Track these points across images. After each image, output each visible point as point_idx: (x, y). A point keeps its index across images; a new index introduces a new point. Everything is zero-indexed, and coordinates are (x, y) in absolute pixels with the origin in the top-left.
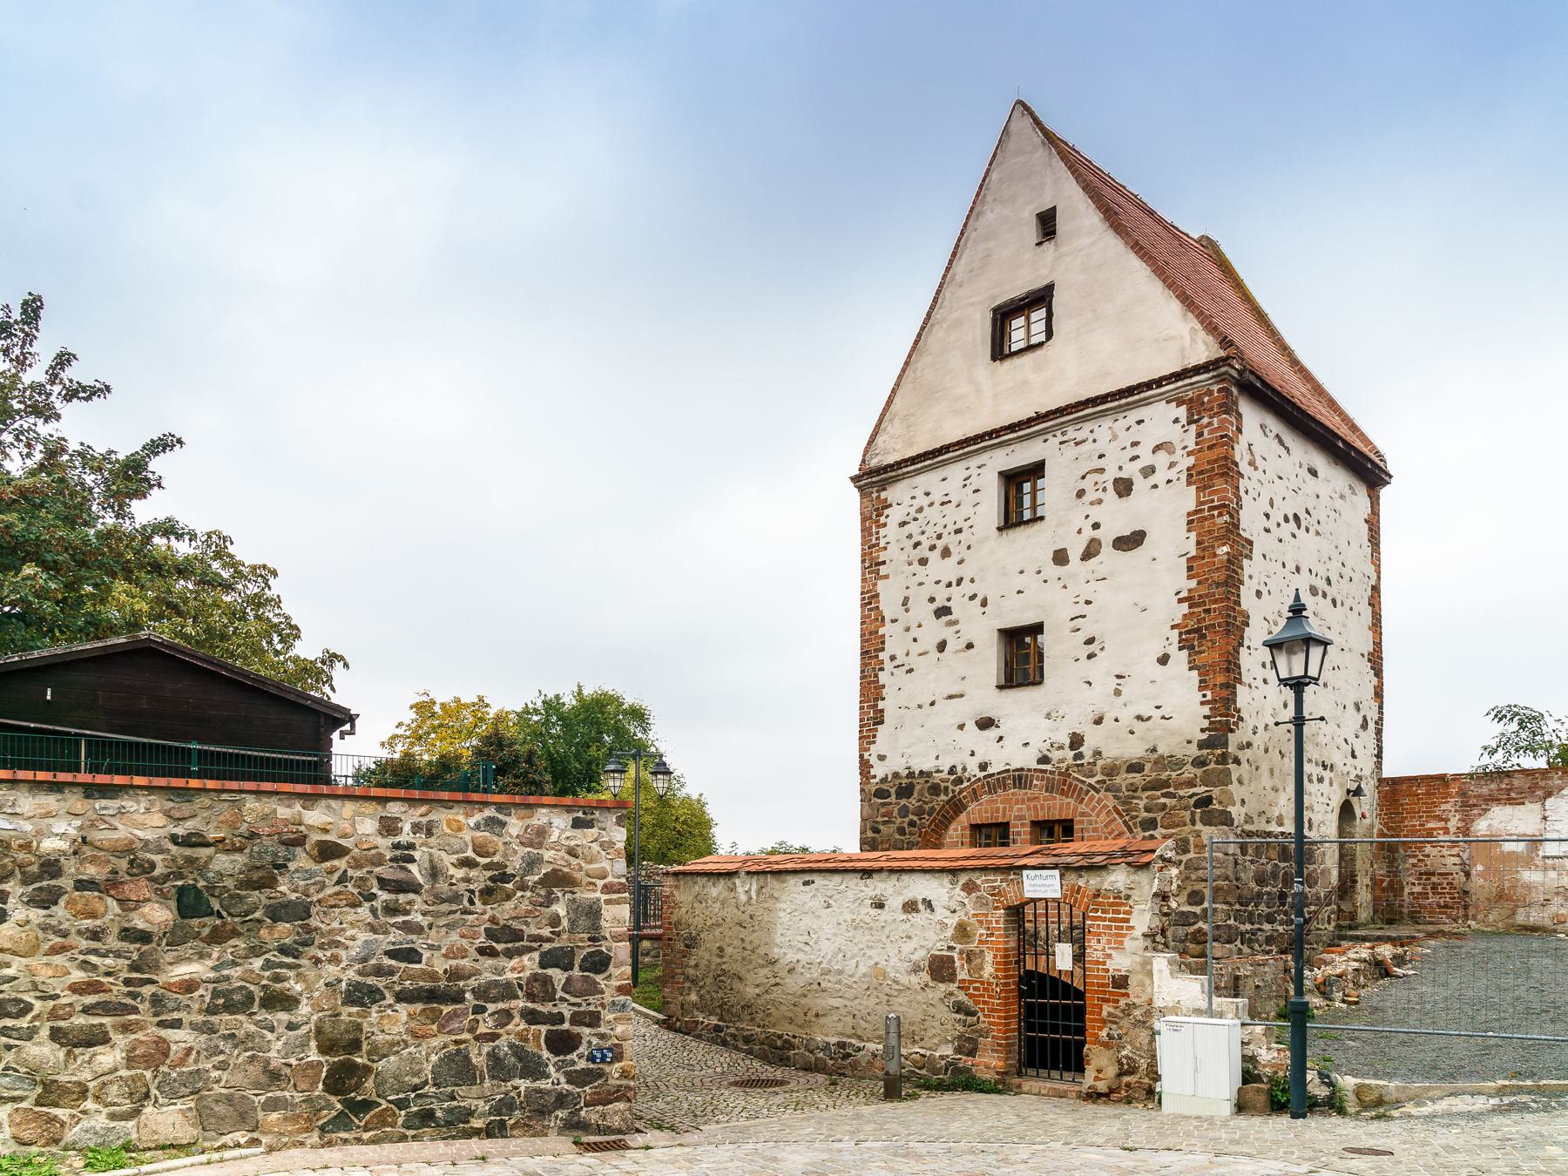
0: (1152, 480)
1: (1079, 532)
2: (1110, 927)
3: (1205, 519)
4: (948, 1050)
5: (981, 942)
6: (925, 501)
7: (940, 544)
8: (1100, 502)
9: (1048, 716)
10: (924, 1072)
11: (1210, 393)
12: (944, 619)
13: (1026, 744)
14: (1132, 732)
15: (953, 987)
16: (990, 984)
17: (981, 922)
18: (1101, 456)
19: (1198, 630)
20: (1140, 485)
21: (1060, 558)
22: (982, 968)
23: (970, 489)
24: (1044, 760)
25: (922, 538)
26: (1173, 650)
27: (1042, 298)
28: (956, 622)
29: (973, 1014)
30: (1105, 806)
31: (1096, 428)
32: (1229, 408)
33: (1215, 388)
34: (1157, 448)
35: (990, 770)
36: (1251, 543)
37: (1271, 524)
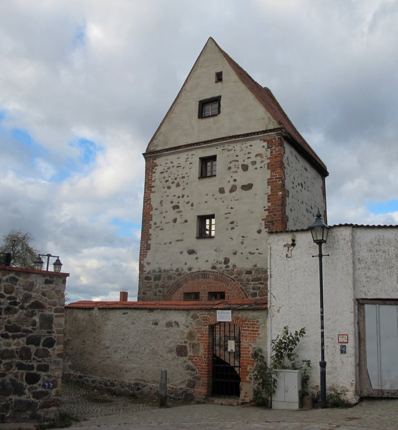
0: (255, 166)
1: (229, 182)
2: (250, 334)
3: (274, 182)
4: (183, 386)
5: (198, 340)
6: (171, 165)
7: (176, 181)
8: (236, 172)
9: (216, 250)
10: (173, 395)
11: (275, 139)
12: (176, 210)
13: (207, 261)
14: (248, 259)
15: (185, 358)
16: (201, 357)
17: (198, 331)
18: (237, 156)
19: (272, 222)
20: (251, 167)
21: (222, 191)
22: (198, 351)
23: (188, 163)
24: (214, 268)
25: (169, 179)
26: (263, 228)
27: (217, 100)
28: (181, 212)
29: (194, 370)
30: (237, 287)
31: (235, 146)
32: (281, 145)
33: (277, 137)
34: (257, 155)
35: (193, 271)
36: (288, 192)
37: (294, 186)
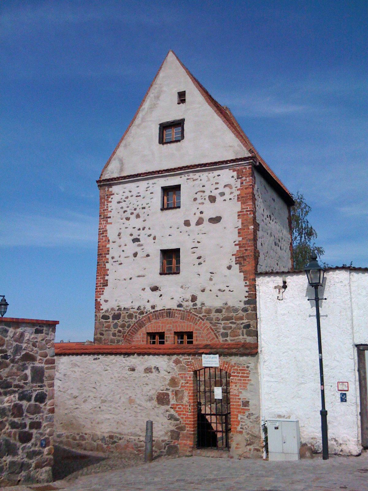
0: (224, 198)
7: (135, 213)
8: (203, 203)
9: (182, 287)
12: (137, 243)
14: (217, 296)
18: (203, 186)
19: (243, 257)
20: (219, 199)
21: (187, 223)
23: (149, 192)
24: (180, 306)
28: (142, 245)
34: (225, 186)
35: (156, 309)
